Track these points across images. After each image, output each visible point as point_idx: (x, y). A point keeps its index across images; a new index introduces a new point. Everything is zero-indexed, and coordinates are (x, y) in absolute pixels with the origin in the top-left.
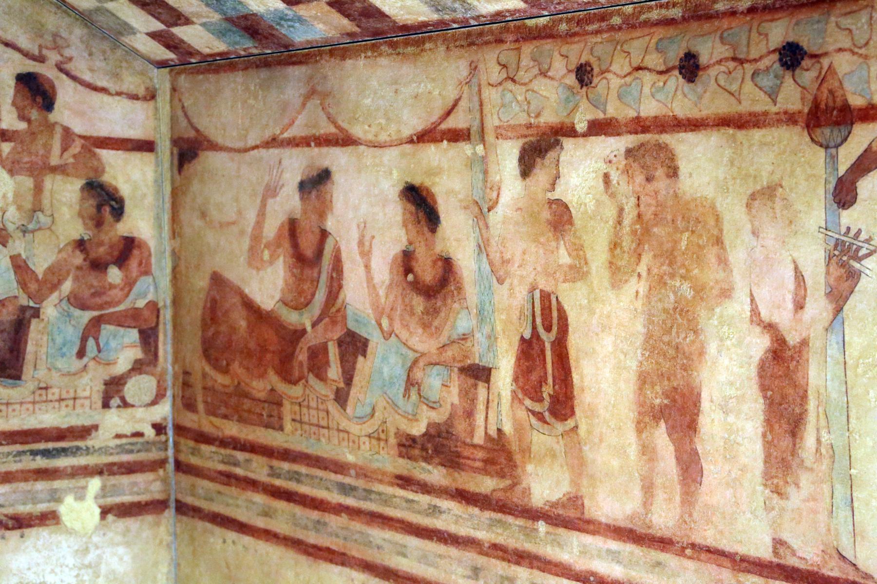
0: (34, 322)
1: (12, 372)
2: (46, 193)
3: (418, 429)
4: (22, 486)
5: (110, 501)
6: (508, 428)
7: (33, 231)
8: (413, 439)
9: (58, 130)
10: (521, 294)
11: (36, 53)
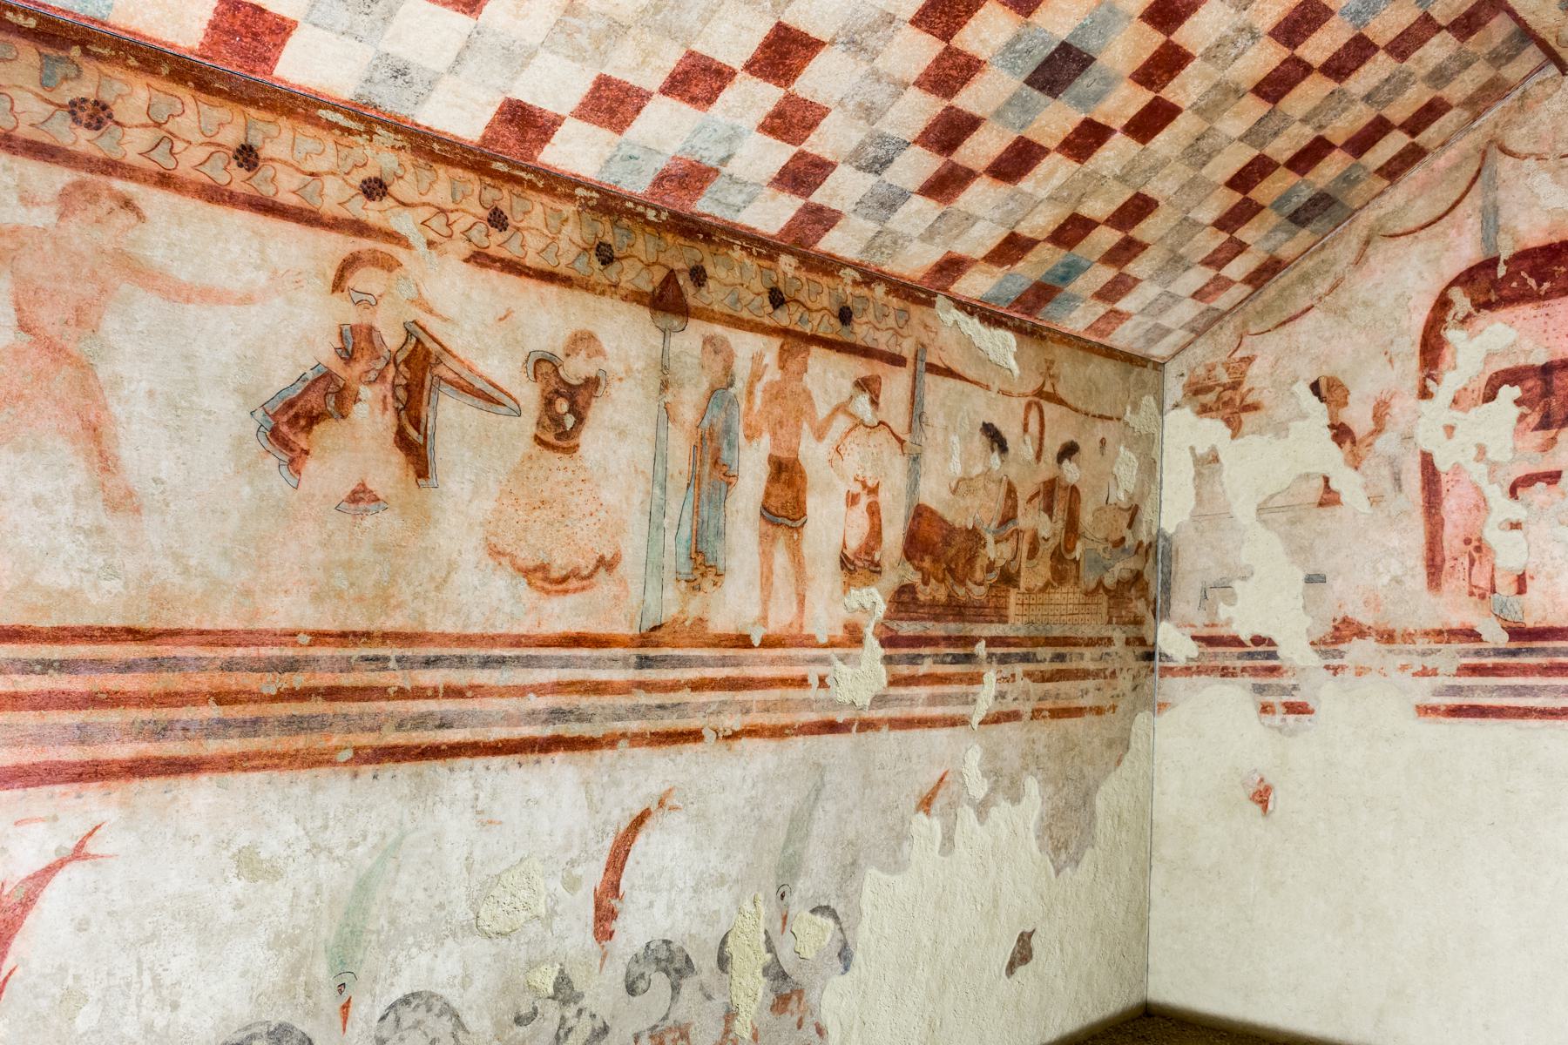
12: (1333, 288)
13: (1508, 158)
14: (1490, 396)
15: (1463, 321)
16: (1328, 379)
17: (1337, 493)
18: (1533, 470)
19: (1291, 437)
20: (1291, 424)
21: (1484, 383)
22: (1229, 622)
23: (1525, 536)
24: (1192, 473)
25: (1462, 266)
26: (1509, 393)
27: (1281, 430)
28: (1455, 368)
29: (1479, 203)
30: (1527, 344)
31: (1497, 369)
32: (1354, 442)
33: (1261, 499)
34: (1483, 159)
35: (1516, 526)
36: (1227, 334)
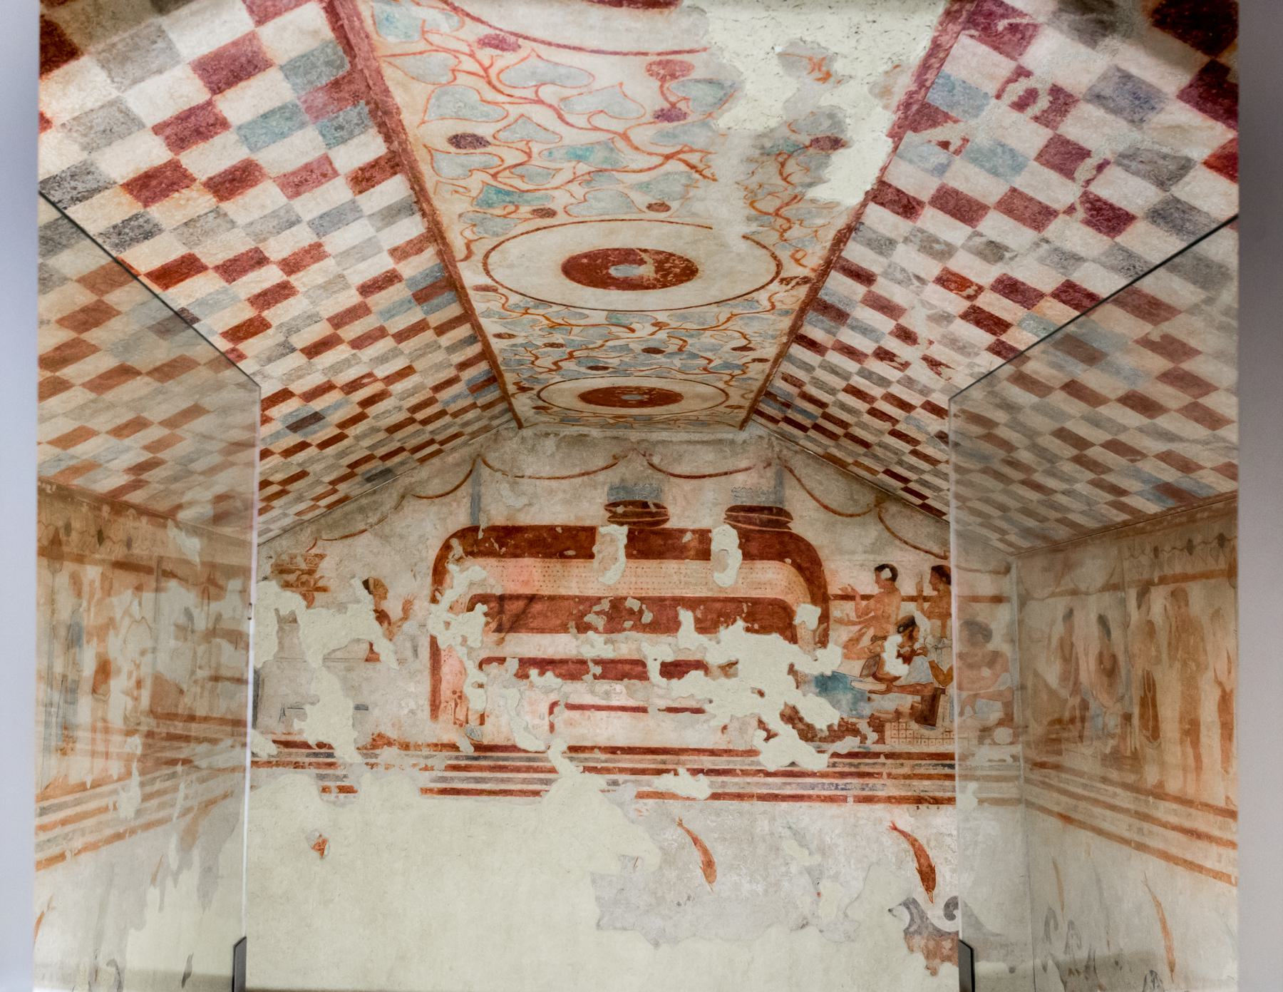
0: (942, 696)
3: (1108, 751)
4: (940, 782)
5: (984, 795)
6: (1138, 747)
8: (1105, 755)
10: (1140, 672)
14: (471, 608)
15: (458, 560)
16: (375, 580)
17: (378, 654)
18: (492, 655)
20: (350, 606)
21: (469, 597)
24: (276, 628)
25: (459, 527)
26: (481, 608)
27: (342, 607)
29: (470, 490)
30: (492, 581)
31: (475, 593)
32: (389, 624)
33: (326, 651)
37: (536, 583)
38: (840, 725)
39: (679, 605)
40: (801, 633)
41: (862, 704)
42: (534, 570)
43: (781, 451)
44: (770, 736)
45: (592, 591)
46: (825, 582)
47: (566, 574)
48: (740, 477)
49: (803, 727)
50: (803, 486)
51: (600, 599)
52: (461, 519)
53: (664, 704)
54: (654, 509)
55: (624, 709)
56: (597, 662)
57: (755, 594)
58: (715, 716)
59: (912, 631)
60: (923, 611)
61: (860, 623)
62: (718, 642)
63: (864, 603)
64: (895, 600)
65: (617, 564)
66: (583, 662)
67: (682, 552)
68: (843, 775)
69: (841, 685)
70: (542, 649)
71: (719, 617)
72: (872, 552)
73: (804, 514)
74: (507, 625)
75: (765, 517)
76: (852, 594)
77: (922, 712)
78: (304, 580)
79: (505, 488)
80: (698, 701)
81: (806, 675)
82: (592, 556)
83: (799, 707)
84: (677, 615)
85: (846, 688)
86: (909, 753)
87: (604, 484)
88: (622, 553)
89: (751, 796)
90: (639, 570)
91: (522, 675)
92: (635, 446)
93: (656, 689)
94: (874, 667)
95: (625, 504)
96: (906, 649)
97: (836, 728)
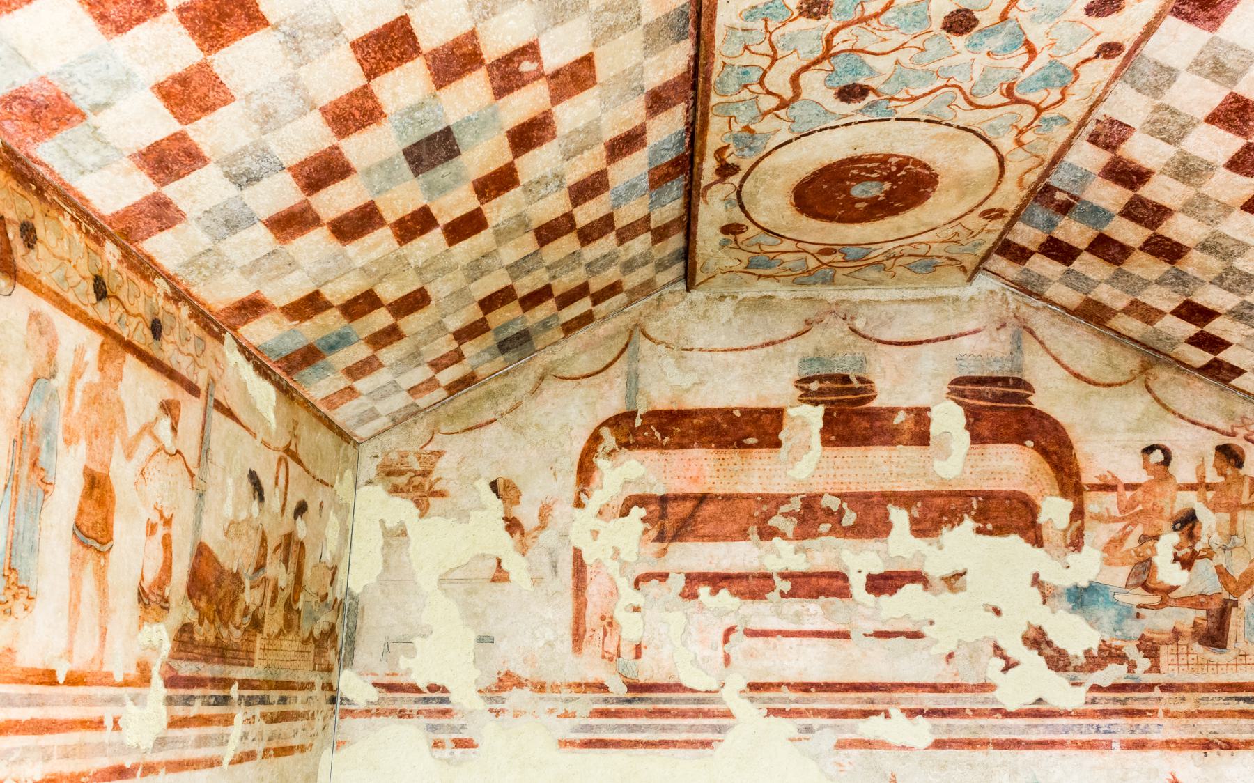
0: (1234, 610)
1: (1220, 643)
2: (1240, 523)
7: (1231, 549)
9: (1247, 481)
11: (1230, 431)
12: (513, 409)
13: (647, 341)
14: (625, 513)
15: (609, 454)
19: (471, 522)
22: (408, 672)
23: (642, 617)
26: (637, 512)
27: (463, 515)
28: (601, 488)
30: (652, 479)
32: (522, 534)
34: (630, 336)
35: (637, 609)
36: (420, 429)
37: (708, 480)
38: (1100, 650)
39: (889, 501)
40: (1046, 533)
41: (1129, 622)
42: (705, 463)
43: (1018, 308)
44: (1009, 665)
45: (777, 488)
46: (1078, 468)
47: (745, 467)
48: (966, 342)
49: (1052, 653)
50: (1047, 350)
51: (789, 497)
52: (614, 404)
53: (871, 627)
54: (856, 384)
55: (819, 634)
56: (785, 576)
57: (987, 486)
58: (937, 642)
59: (1193, 527)
60: (1205, 501)
61: (1123, 519)
62: (941, 548)
63: (1129, 494)
64: (1169, 489)
65: (811, 453)
66: (768, 577)
67: (893, 436)
68: (1105, 714)
69: (1101, 599)
70: (715, 561)
71: (941, 516)
72: (1139, 429)
73: (1050, 385)
74: (670, 532)
75: (999, 390)
76: (1113, 483)
77: (1208, 630)
78: (416, 483)
79: (669, 363)
80: (915, 623)
81: (1056, 587)
82: (778, 444)
83: (1046, 628)
84: (887, 515)
85: (1107, 602)
86: (1193, 684)
87: (794, 355)
88: (816, 438)
89: (985, 743)
90: (838, 460)
91: (689, 594)
92: (834, 308)
93: (861, 608)
94: (1143, 574)
95: (820, 379)
96: (1187, 550)
97: (1095, 653)
